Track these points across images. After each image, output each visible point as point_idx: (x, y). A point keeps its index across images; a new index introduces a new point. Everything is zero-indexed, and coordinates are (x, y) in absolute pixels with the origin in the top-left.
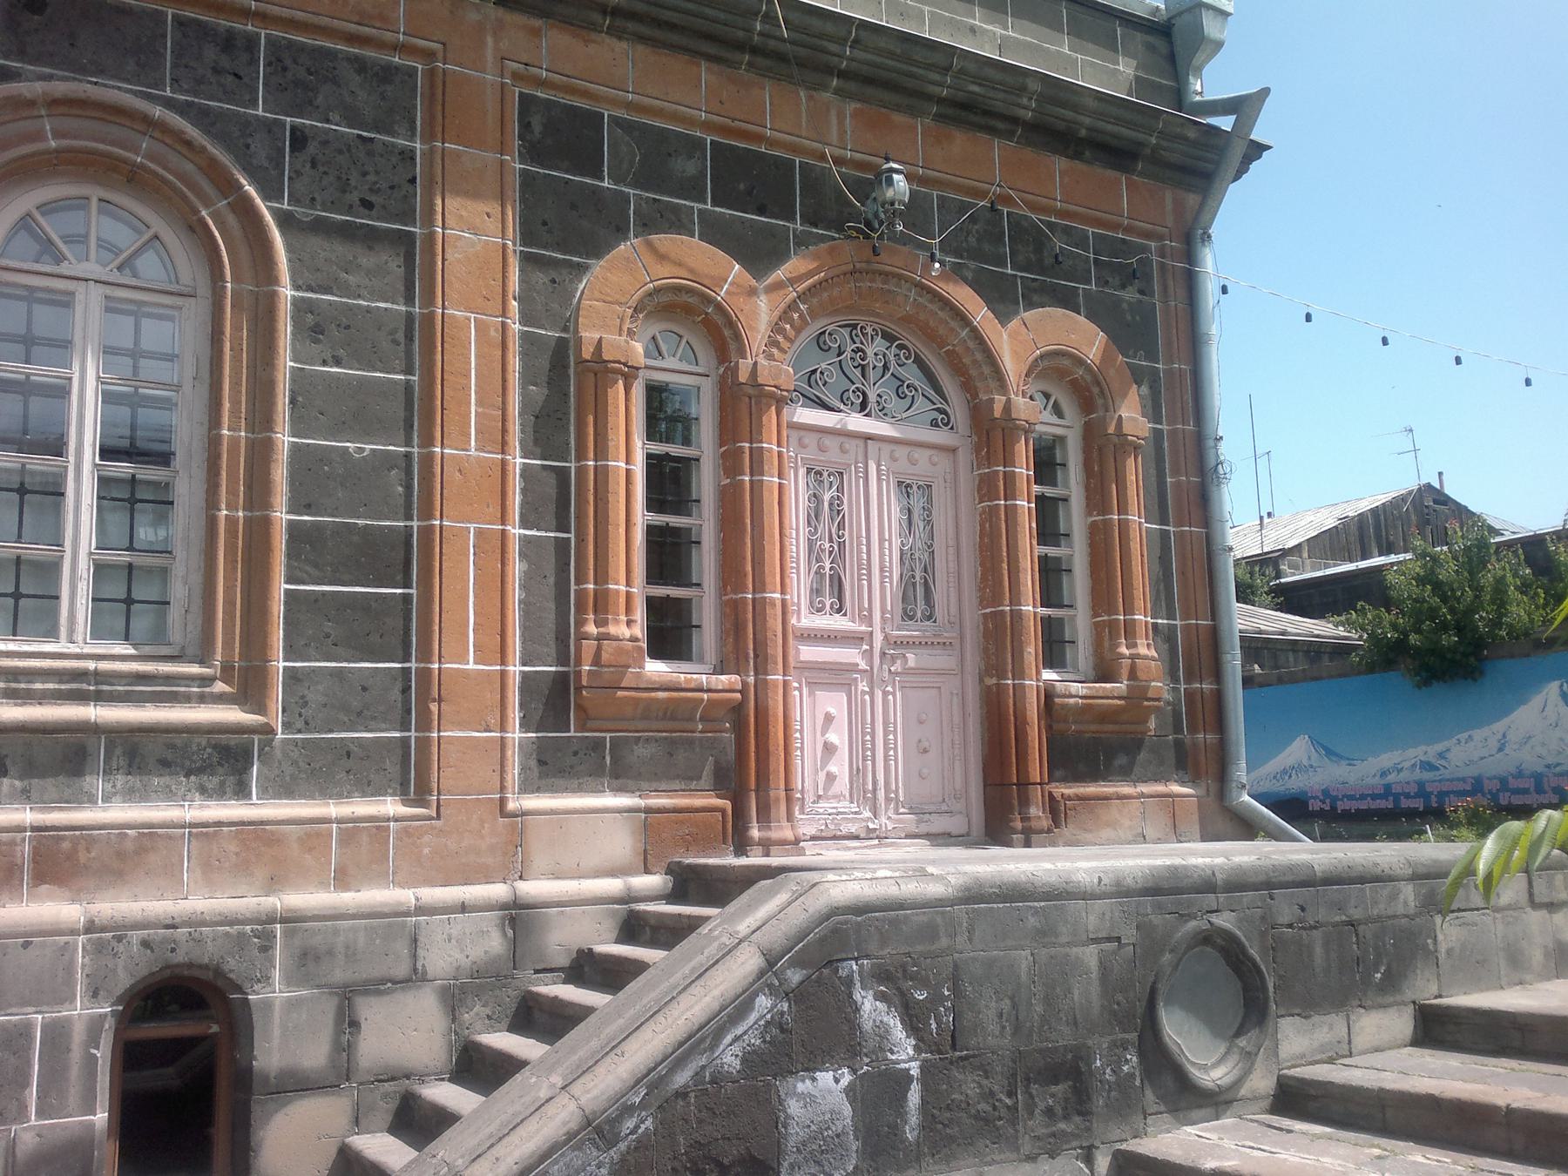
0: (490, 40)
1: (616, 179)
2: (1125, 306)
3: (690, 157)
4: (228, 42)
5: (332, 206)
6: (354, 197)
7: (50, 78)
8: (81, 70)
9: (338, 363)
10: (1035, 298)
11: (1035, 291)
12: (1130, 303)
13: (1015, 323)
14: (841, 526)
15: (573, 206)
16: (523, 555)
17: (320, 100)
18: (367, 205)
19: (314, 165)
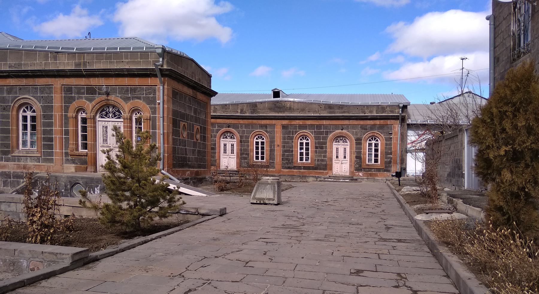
0: (59, 82)
1: (74, 94)
2: (150, 98)
3: (83, 89)
4: (36, 88)
5: (45, 104)
6: (47, 102)
7: (22, 96)
8: (24, 94)
9: (46, 120)
10: (134, 99)
11: (134, 98)
12: (151, 97)
13: (129, 104)
14: (107, 133)
15: (69, 99)
16: (65, 139)
17: (44, 92)
18: (49, 103)
19: (44, 99)
